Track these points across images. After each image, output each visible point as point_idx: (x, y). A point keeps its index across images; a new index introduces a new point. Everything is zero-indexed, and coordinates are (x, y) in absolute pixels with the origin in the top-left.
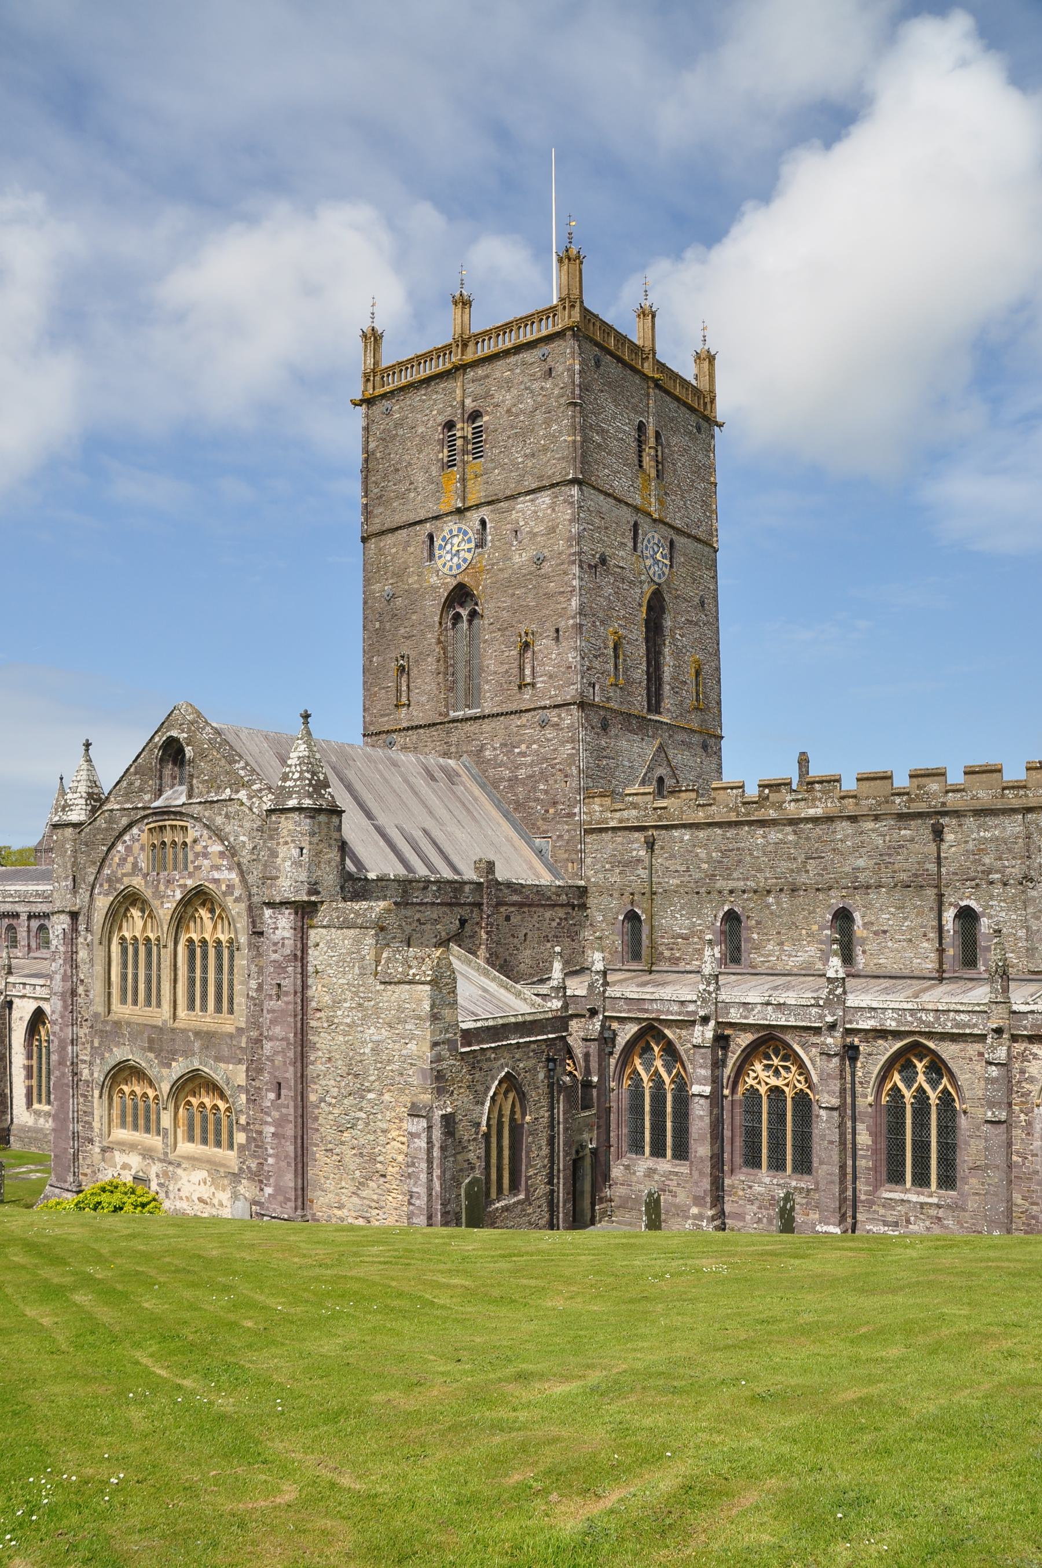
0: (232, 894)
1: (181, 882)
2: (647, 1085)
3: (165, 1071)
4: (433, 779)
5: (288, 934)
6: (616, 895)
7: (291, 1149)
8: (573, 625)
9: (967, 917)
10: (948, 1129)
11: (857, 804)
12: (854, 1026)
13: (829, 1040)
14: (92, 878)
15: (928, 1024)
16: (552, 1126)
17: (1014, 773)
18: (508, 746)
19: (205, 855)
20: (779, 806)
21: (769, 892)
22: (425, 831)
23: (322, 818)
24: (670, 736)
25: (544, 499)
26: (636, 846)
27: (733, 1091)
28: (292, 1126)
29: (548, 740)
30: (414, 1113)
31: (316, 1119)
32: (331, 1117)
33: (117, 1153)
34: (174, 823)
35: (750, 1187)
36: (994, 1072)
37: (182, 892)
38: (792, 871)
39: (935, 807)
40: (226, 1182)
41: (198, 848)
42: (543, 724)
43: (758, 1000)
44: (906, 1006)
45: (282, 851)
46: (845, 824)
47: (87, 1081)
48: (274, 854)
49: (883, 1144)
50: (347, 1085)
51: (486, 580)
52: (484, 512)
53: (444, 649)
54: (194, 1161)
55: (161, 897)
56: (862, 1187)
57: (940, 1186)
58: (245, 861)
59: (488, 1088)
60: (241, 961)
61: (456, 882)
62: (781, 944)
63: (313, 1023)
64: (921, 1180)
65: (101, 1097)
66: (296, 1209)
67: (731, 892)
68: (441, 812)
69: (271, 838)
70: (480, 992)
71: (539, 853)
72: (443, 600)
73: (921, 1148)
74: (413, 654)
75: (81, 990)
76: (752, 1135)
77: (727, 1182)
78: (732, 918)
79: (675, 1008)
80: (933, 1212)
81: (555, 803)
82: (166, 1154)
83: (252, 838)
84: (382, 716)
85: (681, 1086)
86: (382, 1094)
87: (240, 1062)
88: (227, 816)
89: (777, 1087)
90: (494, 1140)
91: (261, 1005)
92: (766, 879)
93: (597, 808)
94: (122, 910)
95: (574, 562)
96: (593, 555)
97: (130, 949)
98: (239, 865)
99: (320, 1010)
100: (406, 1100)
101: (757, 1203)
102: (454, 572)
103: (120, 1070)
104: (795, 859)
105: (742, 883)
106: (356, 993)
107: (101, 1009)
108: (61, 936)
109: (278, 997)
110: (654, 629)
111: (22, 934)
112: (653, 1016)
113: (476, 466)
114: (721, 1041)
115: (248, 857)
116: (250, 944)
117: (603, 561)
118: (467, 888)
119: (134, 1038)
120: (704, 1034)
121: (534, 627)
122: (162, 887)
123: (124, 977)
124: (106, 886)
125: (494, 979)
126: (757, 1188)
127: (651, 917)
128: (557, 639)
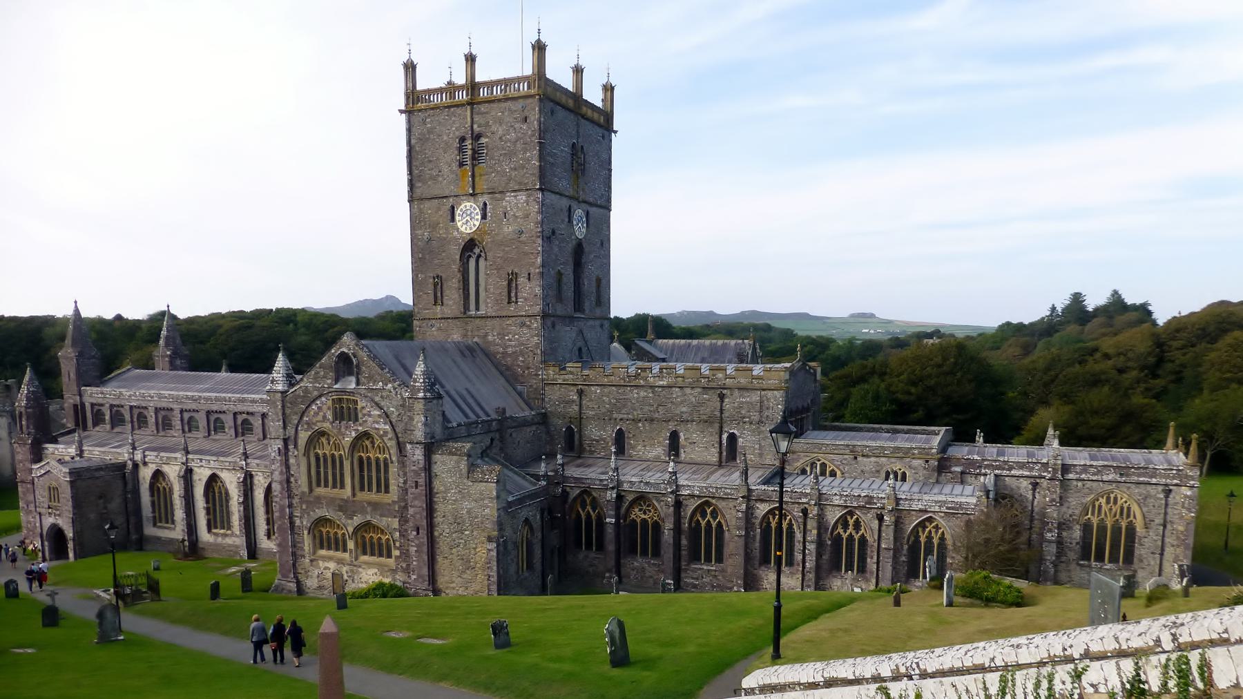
0: (387, 436)
1: (355, 428)
3: (349, 521)
4: (465, 356)
5: (421, 458)
6: (561, 418)
7: (426, 558)
8: (538, 273)
9: (732, 438)
11: (683, 381)
12: (680, 493)
13: (670, 499)
14: (296, 422)
15: (713, 493)
18: (502, 335)
19: (370, 415)
20: (645, 379)
21: (640, 420)
22: (467, 389)
23: (435, 402)
24: (585, 324)
26: (572, 393)
27: (625, 521)
28: (426, 547)
29: (525, 334)
30: (490, 539)
31: (438, 543)
32: (445, 542)
33: (321, 563)
34: (349, 397)
35: (633, 563)
36: (740, 515)
37: (356, 433)
38: (651, 411)
39: (720, 385)
40: (388, 574)
41: (364, 412)
42: (523, 325)
43: (637, 480)
44: (703, 485)
45: (416, 418)
46: (677, 389)
47: (298, 526)
48: (411, 419)
50: (454, 528)
51: (487, 239)
53: (463, 275)
54: (369, 565)
55: (344, 435)
56: (683, 563)
57: (715, 562)
58: (394, 421)
59: (518, 526)
60: (393, 469)
61: (488, 421)
62: (645, 446)
63: (435, 499)
64: (708, 560)
65: (309, 533)
66: (429, 585)
67: (621, 419)
69: (410, 411)
71: (520, 394)
72: (461, 247)
73: (709, 546)
74: (444, 276)
75: (292, 479)
77: (622, 561)
78: (620, 433)
79: (598, 482)
80: (713, 573)
81: (528, 368)
82: (352, 561)
83: (397, 410)
84: (428, 309)
85: (600, 519)
86: (473, 532)
87: (395, 517)
88: (382, 397)
89: (645, 519)
90: (520, 548)
91: (406, 490)
92: (638, 414)
93: (551, 373)
94: (316, 439)
95: (539, 237)
96: (549, 231)
97: (322, 459)
98: (391, 422)
99: (437, 493)
100: (486, 535)
101: (636, 571)
102: (468, 231)
103: (320, 520)
104: (653, 405)
105: (625, 416)
106: (458, 486)
107: (306, 490)
108: (277, 452)
109: (416, 488)
110: (578, 265)
111: (177, 423)
112: (587, 485)
114: (620, 498)
115: (396, 419)
116: (398, 462)
117: (553, 232)
118: (494, 423)
119: (328, 505)
121: (516, 270)
122: (343, 430)
123: (318, 473)
124: (306, 426)
125: (511, 470)
126: (636, 564)
127: (580, 431)
128: (529, 279)
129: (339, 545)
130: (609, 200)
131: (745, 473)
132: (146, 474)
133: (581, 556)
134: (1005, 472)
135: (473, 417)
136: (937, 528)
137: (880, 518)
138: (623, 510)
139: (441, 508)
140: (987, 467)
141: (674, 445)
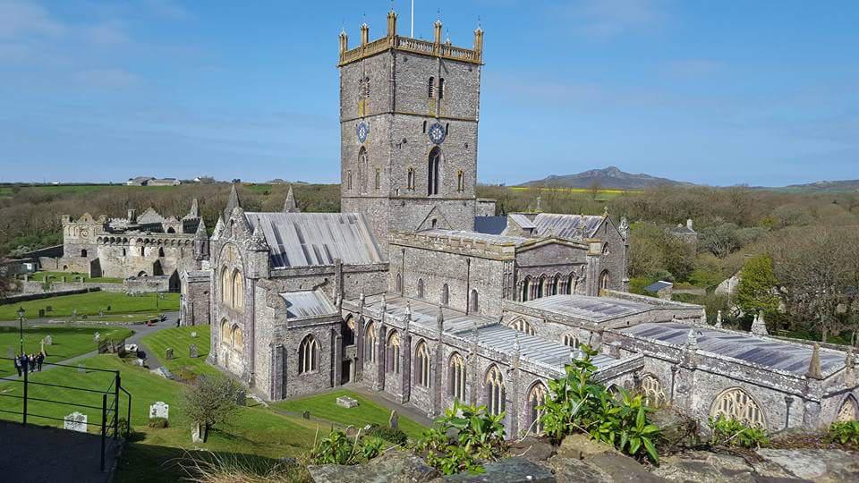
4: (342, 222)
16: (333, 350)
20: (433, 244)
22: (326, 246)
56: (412, 383)
68: (337, 234)
70: (318, 304)
71: (378, 250)
114: (384, 328)
117: (405, 141)
120: (380, 325)
134: (652, 354)
135: (315, 262)
138: (387, 338)
140: (639, 346)
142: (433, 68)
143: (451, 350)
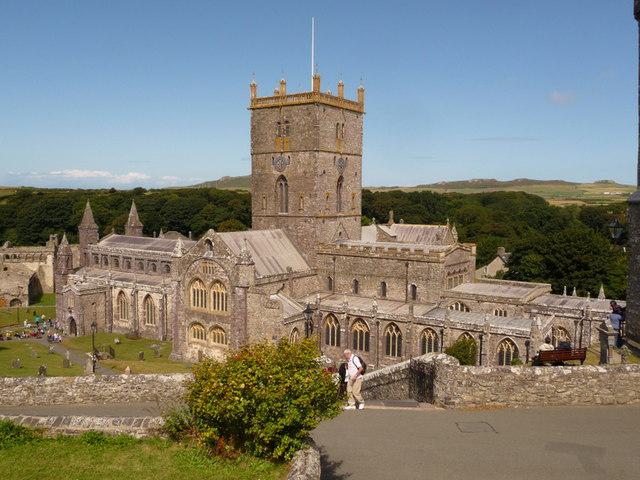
2: (330, 327)
9: (414, 287)
10: (400, 343)
17: (427, 252)
18: (296, 226)
25: (307, 154)
49: (385, 346)
52: (289, 154)
54: (216, 347)
76: (355, 341)
78: (356, 282)
85: (339, 328)
111: (133, 264)
113: (287, 139)
114: (348, 318)
129: (201, 335)
130: (361, 150)
131: (411, 308)
132: (115, 292)
133: (328, 349)
136: (513, 344)
137: (481, 338)
139: (251, 321)
141: (384, 292)
142: (337, 114)
143: (421, 328)
